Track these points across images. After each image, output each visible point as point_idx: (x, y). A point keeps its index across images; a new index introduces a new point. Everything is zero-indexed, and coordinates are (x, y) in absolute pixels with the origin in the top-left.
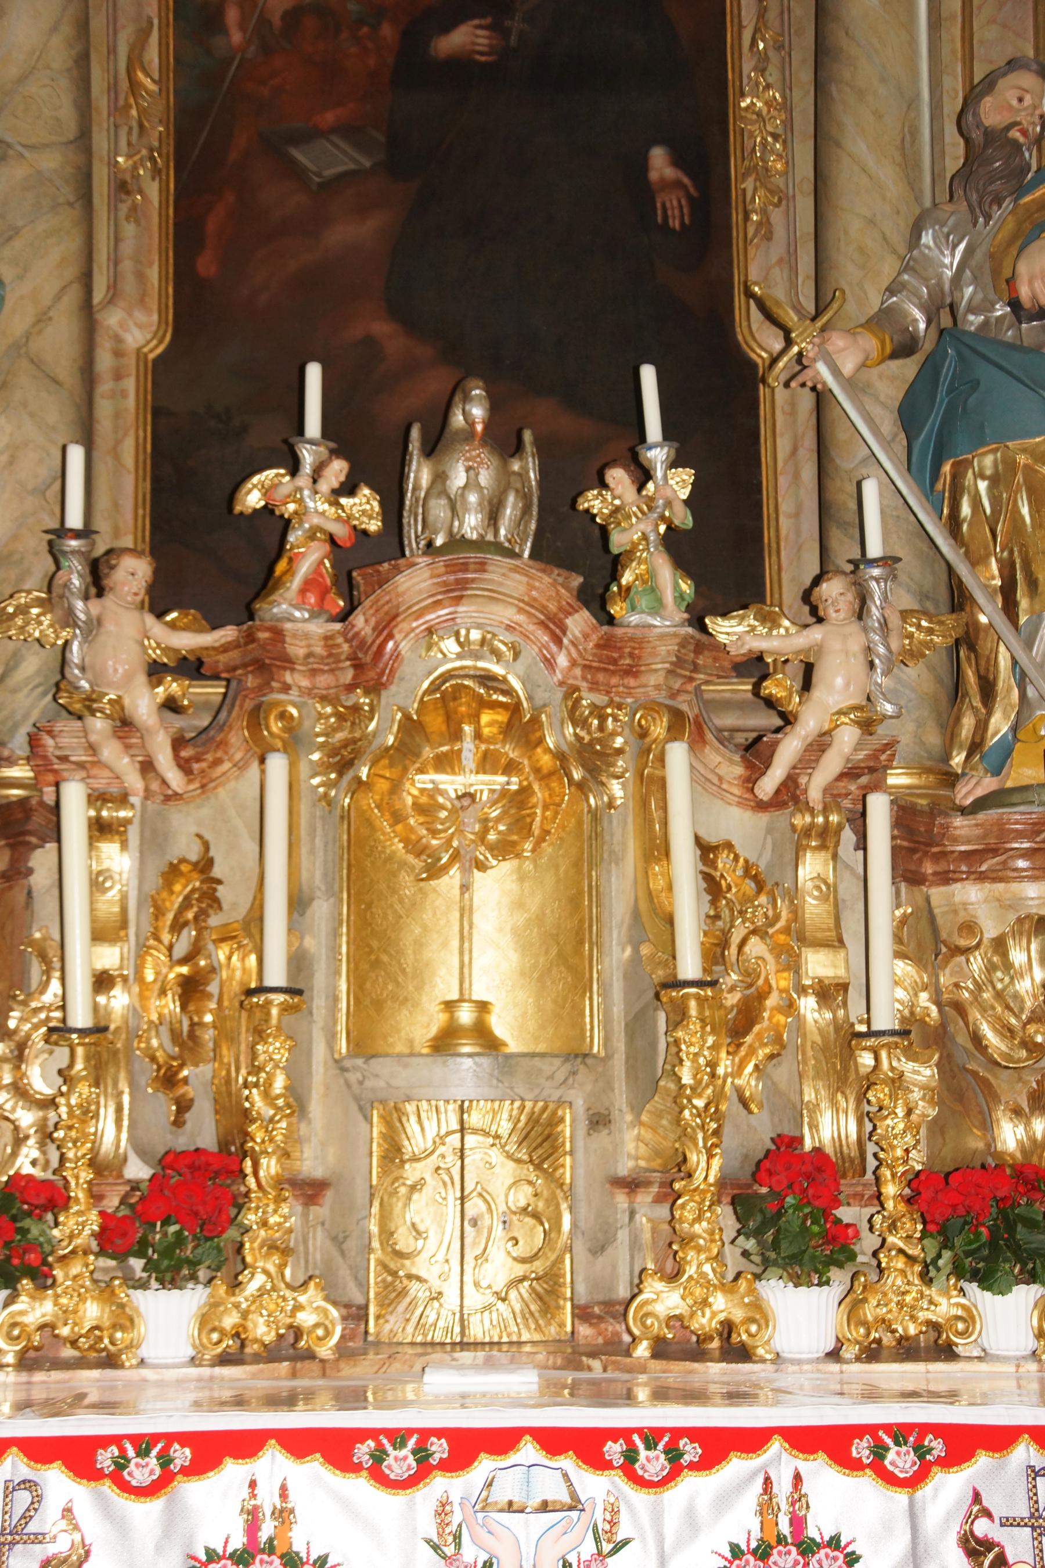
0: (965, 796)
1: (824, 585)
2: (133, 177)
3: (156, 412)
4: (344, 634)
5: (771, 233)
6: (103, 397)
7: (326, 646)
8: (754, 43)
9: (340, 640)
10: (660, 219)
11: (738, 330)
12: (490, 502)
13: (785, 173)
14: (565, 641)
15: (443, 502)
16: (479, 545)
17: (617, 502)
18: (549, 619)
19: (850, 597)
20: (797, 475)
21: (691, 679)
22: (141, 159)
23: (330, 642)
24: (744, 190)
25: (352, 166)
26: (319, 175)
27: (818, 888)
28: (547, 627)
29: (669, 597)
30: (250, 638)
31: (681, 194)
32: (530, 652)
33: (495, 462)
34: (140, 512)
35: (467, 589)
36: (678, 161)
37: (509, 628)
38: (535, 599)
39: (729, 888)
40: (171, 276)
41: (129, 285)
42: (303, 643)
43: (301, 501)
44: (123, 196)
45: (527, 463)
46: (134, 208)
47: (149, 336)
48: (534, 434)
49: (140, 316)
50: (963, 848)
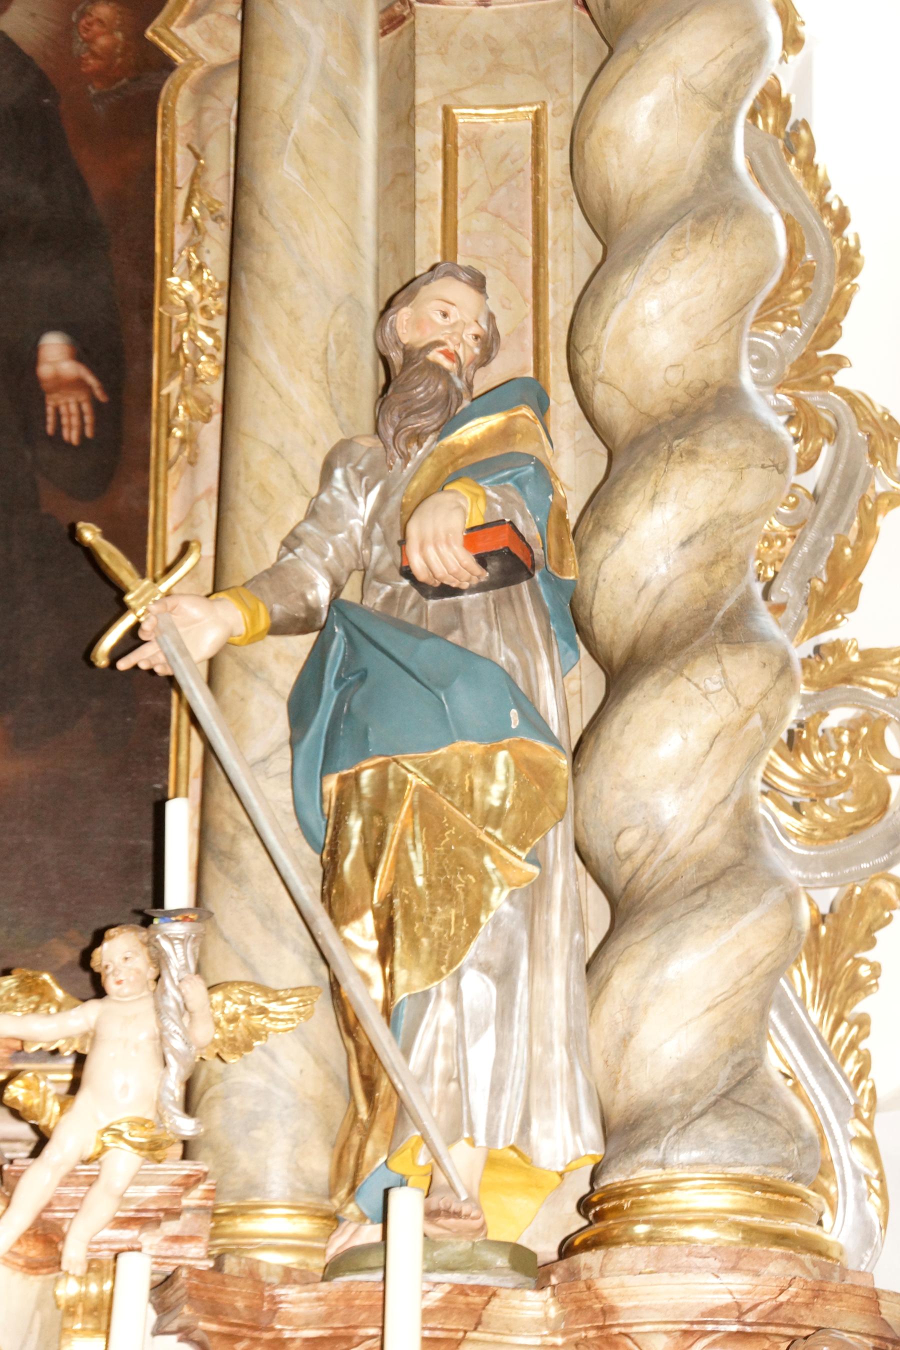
1: (106, 945)
5: (196, 455)
8: (187, 212)
10: (50, 429)
31: (83, 397)
36: (81, 354)
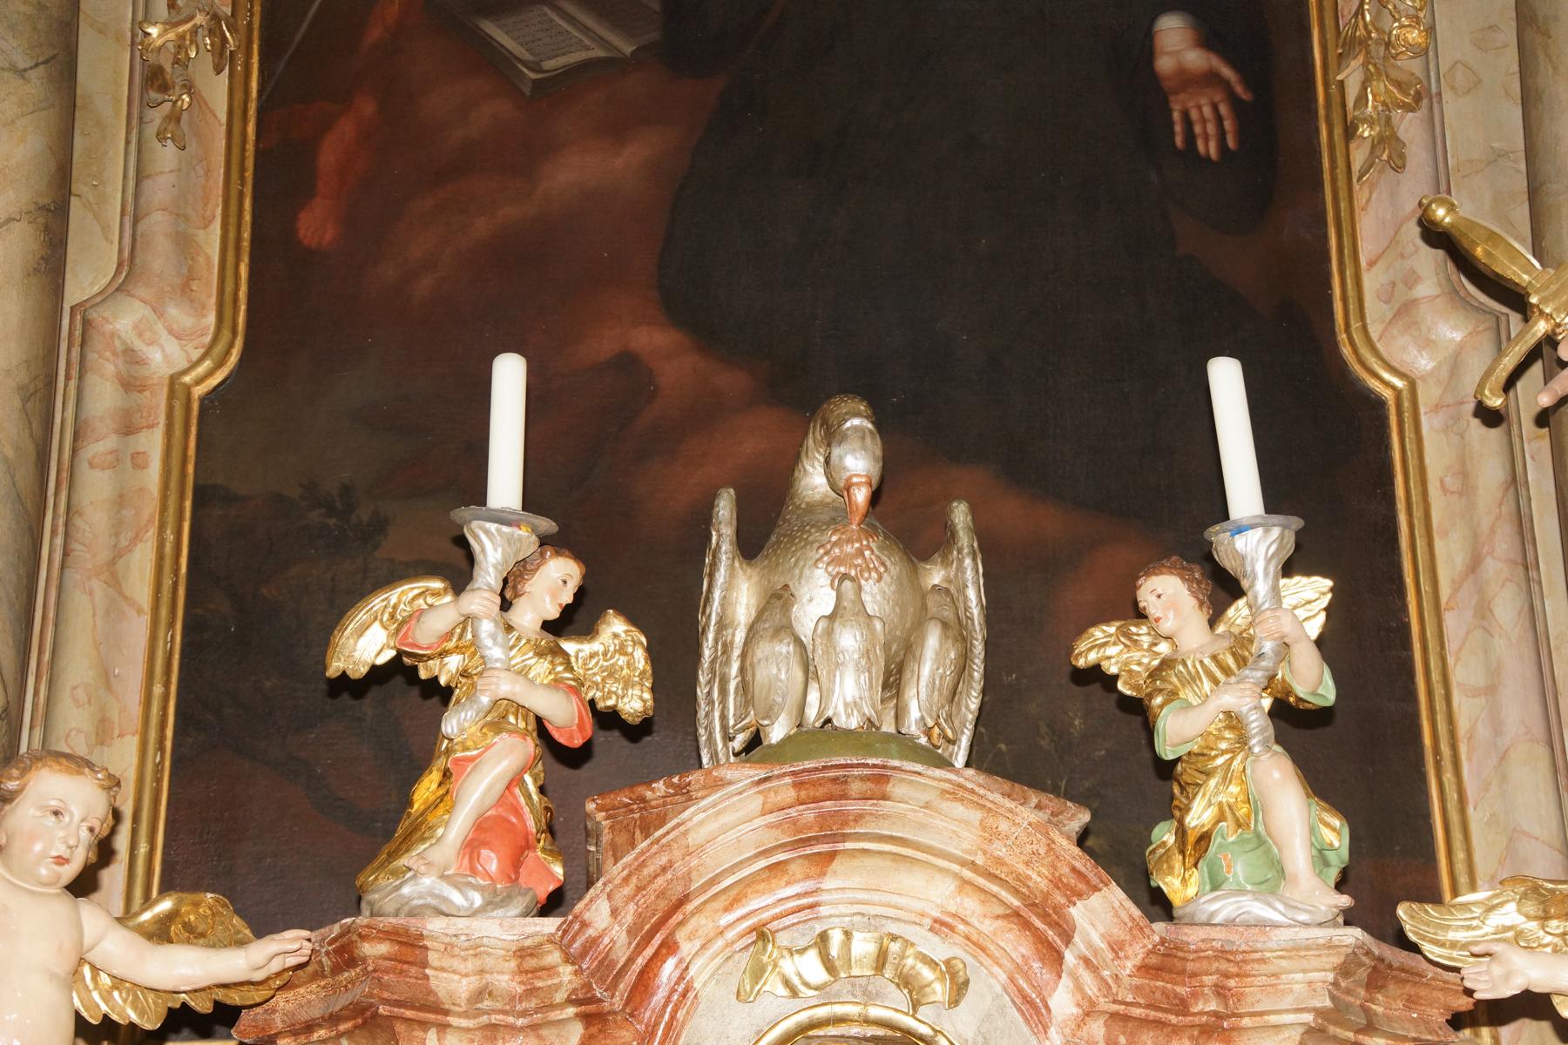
2: (176, 62)
3: (203, 497)
4: (562, 941)
5: (1402, 156)
6: (92, 466)
7: (522, 971)
9: (554, 957)
11: (1342, 337)
12: (886, 647)
13: (1422, 52)
14: (1069, 957)
15: (785, 648)
16: (867, 738)
17: (1164, 648)
18: (1032, 906)
20: (1484, 611)
22: (194, 31)
23: (532, 963)
24: (1342, 83)
25: (599, 53)
26: (536, 68)
28: (1026, 925)
29: (1299, 859)
30: (346, 956)
31: (1218, 97)
32: (988, 985)
33: (894, 566)
34: (158, 689)
35: (845, 838)
36: (1208, 39)
37: (941, 926)
38: (999, 862)
40: (246, 244)
41: (160, 258)
42: (470, 965)
43: (474, 648)
44: (154, 95)
45: (961, 569)
46: (175, 117)
47: (196, 355)
48: (974, 510)
49: (178, 314)
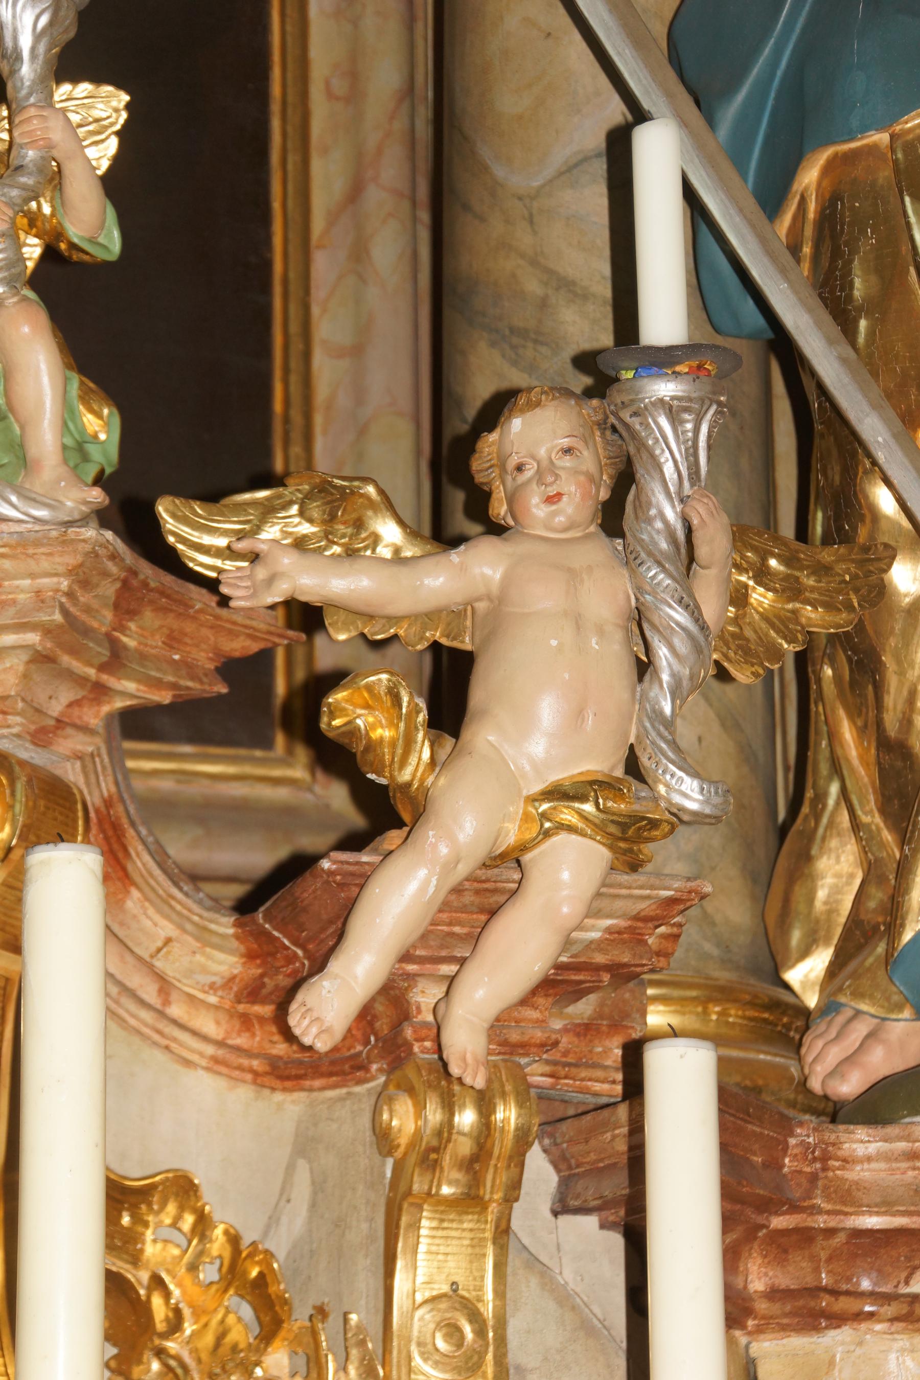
0: (838, 1071)
1: (516, 424)
19: (587, 460)
21: (100, 691)
27: (453, 1332)
39: (176, 1323)
50: (872, 1222)
